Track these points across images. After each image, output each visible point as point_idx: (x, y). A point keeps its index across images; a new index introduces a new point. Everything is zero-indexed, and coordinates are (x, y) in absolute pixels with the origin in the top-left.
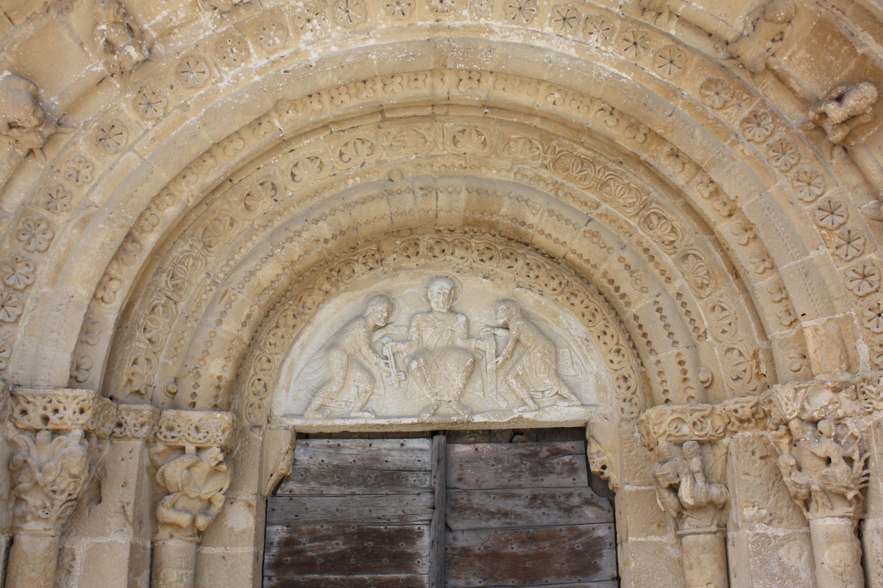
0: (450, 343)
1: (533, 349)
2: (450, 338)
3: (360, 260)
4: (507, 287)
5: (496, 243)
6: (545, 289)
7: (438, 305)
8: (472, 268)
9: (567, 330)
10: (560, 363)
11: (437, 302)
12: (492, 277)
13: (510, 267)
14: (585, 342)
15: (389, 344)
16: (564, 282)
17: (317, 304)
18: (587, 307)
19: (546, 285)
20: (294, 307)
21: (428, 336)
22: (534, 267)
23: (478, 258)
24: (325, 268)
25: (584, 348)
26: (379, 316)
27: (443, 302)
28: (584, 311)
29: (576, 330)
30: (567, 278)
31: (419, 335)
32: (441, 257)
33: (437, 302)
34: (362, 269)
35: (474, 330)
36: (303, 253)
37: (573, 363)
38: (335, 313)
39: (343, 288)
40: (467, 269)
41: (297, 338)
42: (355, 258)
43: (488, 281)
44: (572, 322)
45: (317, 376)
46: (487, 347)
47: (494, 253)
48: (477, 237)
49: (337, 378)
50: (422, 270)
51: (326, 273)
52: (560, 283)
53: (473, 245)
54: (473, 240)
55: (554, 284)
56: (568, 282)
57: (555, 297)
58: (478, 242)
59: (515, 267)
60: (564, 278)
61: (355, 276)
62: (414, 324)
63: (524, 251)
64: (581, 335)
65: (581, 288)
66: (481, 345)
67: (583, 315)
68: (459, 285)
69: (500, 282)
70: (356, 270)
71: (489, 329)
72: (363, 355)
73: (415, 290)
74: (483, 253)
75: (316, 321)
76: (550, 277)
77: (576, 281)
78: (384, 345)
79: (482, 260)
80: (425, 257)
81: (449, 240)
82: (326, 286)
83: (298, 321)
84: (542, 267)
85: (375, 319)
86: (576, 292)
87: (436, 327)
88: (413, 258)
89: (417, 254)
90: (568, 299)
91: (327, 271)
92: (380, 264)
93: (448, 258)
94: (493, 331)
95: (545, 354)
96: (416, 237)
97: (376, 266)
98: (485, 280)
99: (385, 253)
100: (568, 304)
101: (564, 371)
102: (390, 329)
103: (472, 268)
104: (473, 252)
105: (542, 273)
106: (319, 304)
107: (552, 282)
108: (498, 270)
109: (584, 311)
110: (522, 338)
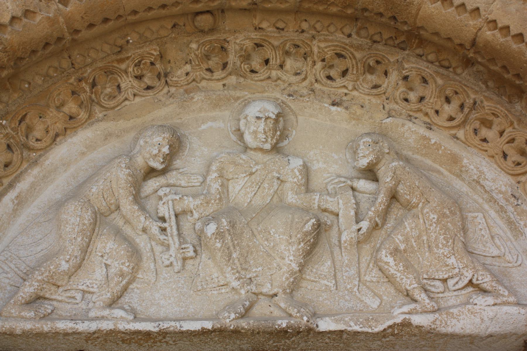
0: (275, 199)
1: (422, 208)
2: (276, 192)
3: (130, 69)
4: (371, 118)
5: (352, 46)
6: (436, 119)
7: (256, 138)
8: (313, 90)
9: (478, 182)
10: (470, 234)
11: (255, 133)
12: (345, 105)
13: (376, 87)
14: (512, 199)
15: (169, 197)
16: (469, 102)
17: (52, 133)
18: (512, 141)
19: (437, 112)
20: (9, 130)
21: (238, 188)
22: (417, 83)
23: (322, 76)
24: (69, 76)
25: (510, 209)
26: (155, 152)
27: (265, 133)
28: (506, 148)
29: (494, 181)
30: (473, 96)
31: (222, 185)
32: (263, 73)
33: (255, 133)
34: (133, 87)
35: (317, 182)
36: (19, 14)
37: (492, 237)
38: (83, 154)
39: (101, 115)
40: (305, 92)
41: (11, 186)
42: (123, 66)
43: (339, 109)
44: (485, 170)
45: (39, 249)
46: (341, 206)
47: (349, 63)
48: (322, 38)
49: (70, 248)
50: (232, 93)
51: (72, 84)
52: (462, 106)
53: (315, 50)
54: (315, 42)
55: (449, 109)
56: (475, 103)
57: (453, 132)
58: (322, 45)
59: (385, 85)
60: (468, 97)
61: (120, 98)
62: (214, 168)
63: (399, 57)
64: (503, 189)
65: (500, 109)
66: (330, 203)
67: (505, 156)
68: (292, 117)
69: (359, 111)
70: (123, 86)
71: (343, 179)
72: (124, 217)
73: (220, 124)
74: (331, 67)
75: (47, 162)
76: (443, 99)
77: (487, 98)
78: (160, 198)
79: (329, 78)
80: (236, 72)
81: (276, 43)
82: (71, 107)
83: (16, 157)
84: (430, 81)
85: (148, 156)
86: (491, 118)
87: (251, 174)
88: (218, 74)
89: (225, 66)
90: (476, 131)
91: (72, 80)
92: (163, 80)
93: (274, 73)
94: (349, 182)
95: (444, 215)
96: (223, 36)
97: (156, 83)
98: (334, 109)
99: (173, 64)
100: (476, 141)
101: (479, 248)
102: (172, 177)
103: (313, 90)
104: (314, 63)
105: (429, 91)
106: (57, 135)
107: (446, 107)
108: (355, 93)
109: (506, 148)
110: (401, 189)
